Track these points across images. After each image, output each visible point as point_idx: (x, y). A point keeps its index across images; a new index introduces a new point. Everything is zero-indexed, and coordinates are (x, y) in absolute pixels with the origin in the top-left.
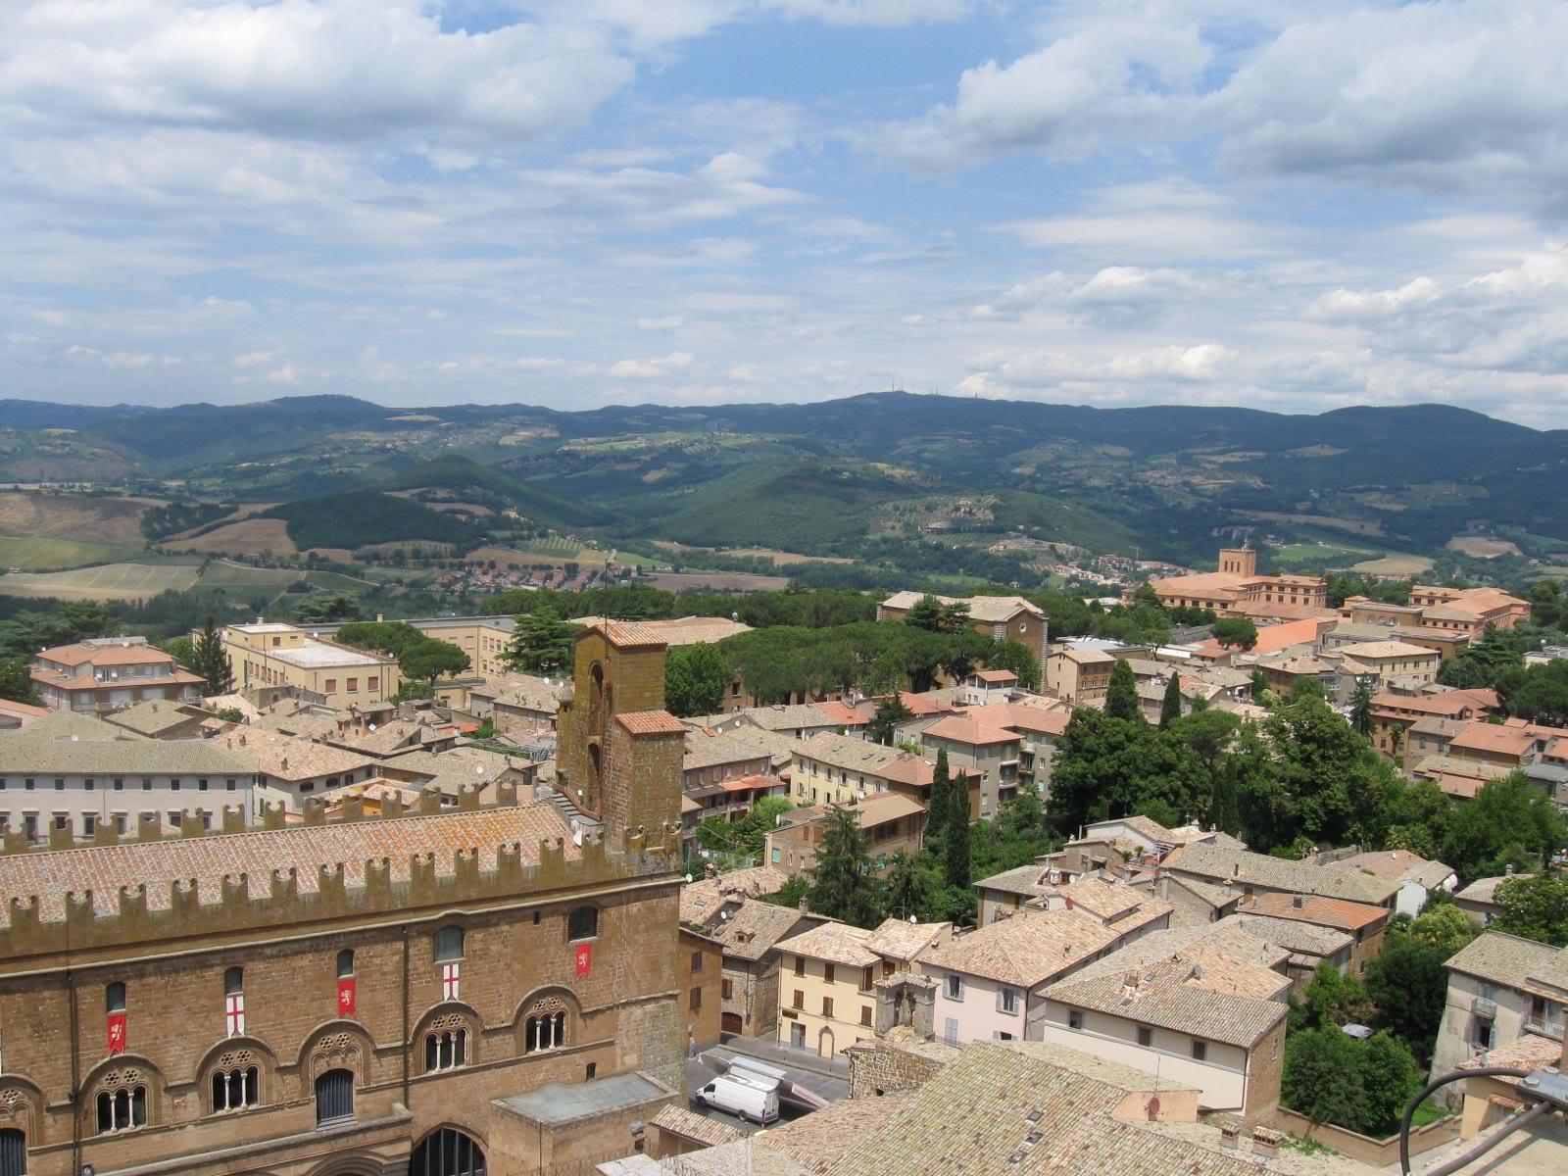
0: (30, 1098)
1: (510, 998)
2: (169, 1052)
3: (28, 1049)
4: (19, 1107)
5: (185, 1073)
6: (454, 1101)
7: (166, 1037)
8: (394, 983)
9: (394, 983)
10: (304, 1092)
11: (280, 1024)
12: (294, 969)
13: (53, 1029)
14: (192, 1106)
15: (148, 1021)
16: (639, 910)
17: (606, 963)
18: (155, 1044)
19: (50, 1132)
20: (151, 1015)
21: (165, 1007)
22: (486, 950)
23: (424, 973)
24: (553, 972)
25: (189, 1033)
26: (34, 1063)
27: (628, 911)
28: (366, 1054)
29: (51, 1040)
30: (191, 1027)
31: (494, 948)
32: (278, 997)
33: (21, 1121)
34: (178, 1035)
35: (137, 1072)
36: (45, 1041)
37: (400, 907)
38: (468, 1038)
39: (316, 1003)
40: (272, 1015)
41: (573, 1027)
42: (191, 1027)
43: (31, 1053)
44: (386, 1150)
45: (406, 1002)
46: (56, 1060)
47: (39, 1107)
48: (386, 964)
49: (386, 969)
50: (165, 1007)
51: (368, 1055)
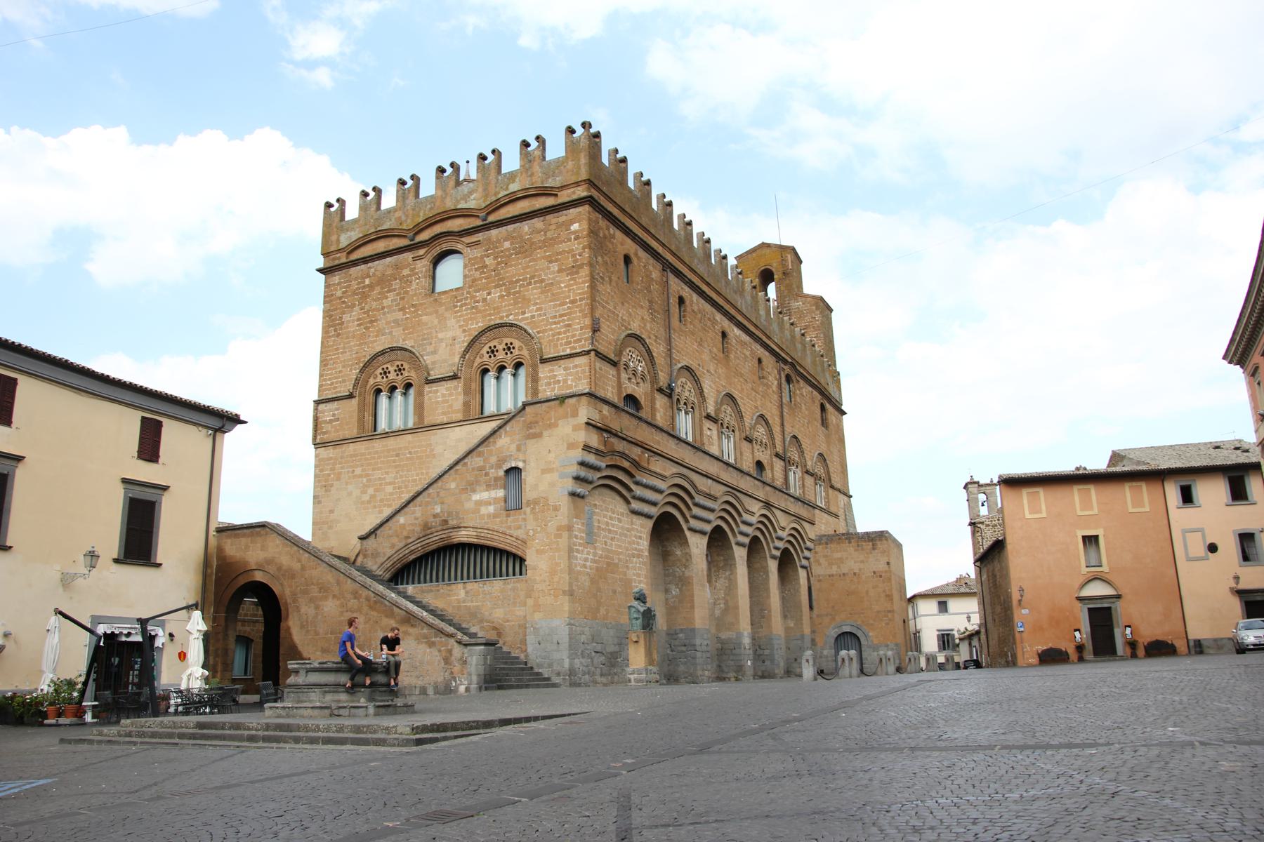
45: (783, 425)
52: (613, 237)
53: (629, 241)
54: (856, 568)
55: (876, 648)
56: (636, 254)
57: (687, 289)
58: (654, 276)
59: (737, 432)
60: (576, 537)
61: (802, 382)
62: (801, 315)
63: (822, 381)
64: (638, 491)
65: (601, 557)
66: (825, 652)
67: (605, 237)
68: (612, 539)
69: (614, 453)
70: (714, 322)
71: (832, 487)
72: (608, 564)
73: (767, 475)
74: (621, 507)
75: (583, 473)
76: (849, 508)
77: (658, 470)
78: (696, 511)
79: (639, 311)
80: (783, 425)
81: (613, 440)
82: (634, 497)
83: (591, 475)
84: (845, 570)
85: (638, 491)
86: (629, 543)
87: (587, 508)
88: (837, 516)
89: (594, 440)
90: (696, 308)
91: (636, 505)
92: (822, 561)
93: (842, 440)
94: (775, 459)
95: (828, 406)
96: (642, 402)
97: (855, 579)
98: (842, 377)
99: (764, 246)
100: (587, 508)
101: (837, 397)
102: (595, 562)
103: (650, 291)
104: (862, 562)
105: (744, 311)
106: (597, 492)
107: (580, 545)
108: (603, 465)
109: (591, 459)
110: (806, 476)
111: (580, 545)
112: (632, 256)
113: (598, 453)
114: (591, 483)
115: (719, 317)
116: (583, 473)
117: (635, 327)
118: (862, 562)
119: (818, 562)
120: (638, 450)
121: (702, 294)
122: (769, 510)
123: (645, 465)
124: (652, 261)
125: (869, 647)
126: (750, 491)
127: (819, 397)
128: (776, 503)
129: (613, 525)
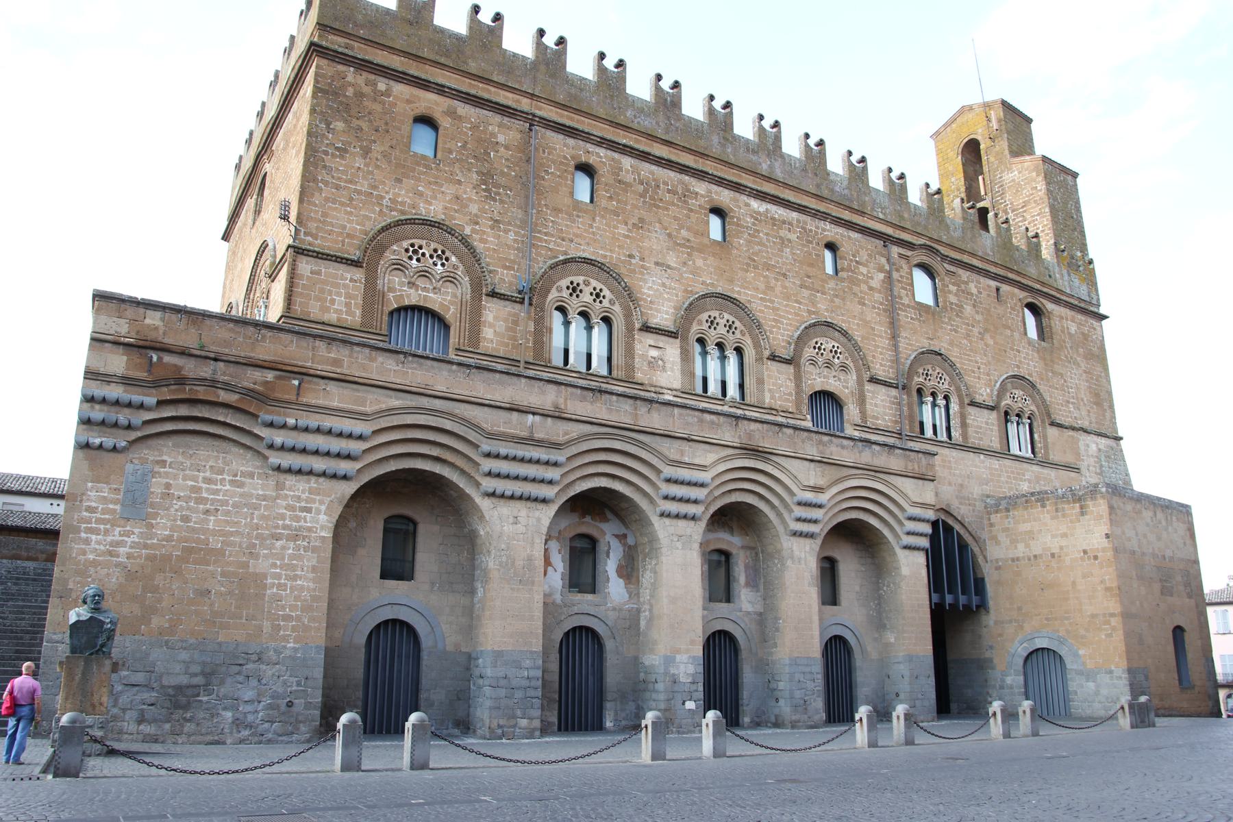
0: (468, 271)
2: (645, 281)
3: (470, 199)
4: (450, 279)
5: (663, 316)
6: (950, 484)
8: (881, 304)
10: (798, 404)
12: (781, 238)
13: (505, 188)
14: (672, 370)
15: (622, 230)
18: (631, 264)
19: (488, 333)
20: (626, 224)
21: (641, 220)
25: (669, 267)
26: (477, 223)
28: (860, 382)
29: (502, 202)
30: (672, 260)
32: (768, 267)
33: (444, 299)
34: (657, 264)
36: (495, 200)
37: (881, 216)
38: (954, 407)
39: (806, 293)
40: (762, 286)
41: (1045, 437)
43: (474, 208)
45: (894, 337)
46: (506, 231)
47: (477, 286)
50: (641, 220)
51: (863, 385)
52: (388, 93)
53: (432, 96)
54: (1054, 544)
55: (1089, 675)
56: (451, 113)
57: (602, 152)
58: (501, 138)
59: (750, 353)
60: (91, 510)
61: (964, 274)
62: (1018, 188)
63: (1032, 271)
64: (279, 438)
65: (169, 539)
66: (1009, 680)
67: (360, 95)
68: (207, 512)
69: (181, 381)
70: (687, 194)
71: (1053, 424)
72: (188, 551)
73: (852, 411)
74: (241, 463)
75: (98, 413)
76: (1115, 456)
77: (335, 404)
78: (488, 465)
79: (450, 190)
80: (894, 337)
81: (168, 359)
82: (271, 446)
83: (123, 417)
84: (1036, 549)
85: (279, 438)
86: (263, 517)
87: (129, 467)
88: (1077, 470)
89: (117, 363)
90: (629, 178)
91: (275, 459)
92: (1002, 537)
93: (1098, 357)
94: (869, 387)
95: (1050, 306)
96: (450, 315)
97: (1054, 564)
98: (1098, 267)
99: (963, 111)
100: (129, 467)
101: (1083, 292)
102: (146, 546)
103: (483, 157)
104: (1064, 535)
105: (779, 174)
106: (170, 442)
107: (99, 521)
108: (151, 400)
109: (115, 392)
110: (971, 410)
111: (99, 521)
112: (437, 115)
113: (127, 381)
114: (129, 427)
115: (701, 187)
116: (98, 413)
117: (434, 209)
118: (1064, 535)
119: (994, 538)
120: (270, 376)
121: (645, 156)
122: (767, 460)
123: (293, 397)
124: (497, 118)
125: (1080, 673)
126: (681, 431)
127: (1022, 294)
128: (782, 448)
129: (216, 492)
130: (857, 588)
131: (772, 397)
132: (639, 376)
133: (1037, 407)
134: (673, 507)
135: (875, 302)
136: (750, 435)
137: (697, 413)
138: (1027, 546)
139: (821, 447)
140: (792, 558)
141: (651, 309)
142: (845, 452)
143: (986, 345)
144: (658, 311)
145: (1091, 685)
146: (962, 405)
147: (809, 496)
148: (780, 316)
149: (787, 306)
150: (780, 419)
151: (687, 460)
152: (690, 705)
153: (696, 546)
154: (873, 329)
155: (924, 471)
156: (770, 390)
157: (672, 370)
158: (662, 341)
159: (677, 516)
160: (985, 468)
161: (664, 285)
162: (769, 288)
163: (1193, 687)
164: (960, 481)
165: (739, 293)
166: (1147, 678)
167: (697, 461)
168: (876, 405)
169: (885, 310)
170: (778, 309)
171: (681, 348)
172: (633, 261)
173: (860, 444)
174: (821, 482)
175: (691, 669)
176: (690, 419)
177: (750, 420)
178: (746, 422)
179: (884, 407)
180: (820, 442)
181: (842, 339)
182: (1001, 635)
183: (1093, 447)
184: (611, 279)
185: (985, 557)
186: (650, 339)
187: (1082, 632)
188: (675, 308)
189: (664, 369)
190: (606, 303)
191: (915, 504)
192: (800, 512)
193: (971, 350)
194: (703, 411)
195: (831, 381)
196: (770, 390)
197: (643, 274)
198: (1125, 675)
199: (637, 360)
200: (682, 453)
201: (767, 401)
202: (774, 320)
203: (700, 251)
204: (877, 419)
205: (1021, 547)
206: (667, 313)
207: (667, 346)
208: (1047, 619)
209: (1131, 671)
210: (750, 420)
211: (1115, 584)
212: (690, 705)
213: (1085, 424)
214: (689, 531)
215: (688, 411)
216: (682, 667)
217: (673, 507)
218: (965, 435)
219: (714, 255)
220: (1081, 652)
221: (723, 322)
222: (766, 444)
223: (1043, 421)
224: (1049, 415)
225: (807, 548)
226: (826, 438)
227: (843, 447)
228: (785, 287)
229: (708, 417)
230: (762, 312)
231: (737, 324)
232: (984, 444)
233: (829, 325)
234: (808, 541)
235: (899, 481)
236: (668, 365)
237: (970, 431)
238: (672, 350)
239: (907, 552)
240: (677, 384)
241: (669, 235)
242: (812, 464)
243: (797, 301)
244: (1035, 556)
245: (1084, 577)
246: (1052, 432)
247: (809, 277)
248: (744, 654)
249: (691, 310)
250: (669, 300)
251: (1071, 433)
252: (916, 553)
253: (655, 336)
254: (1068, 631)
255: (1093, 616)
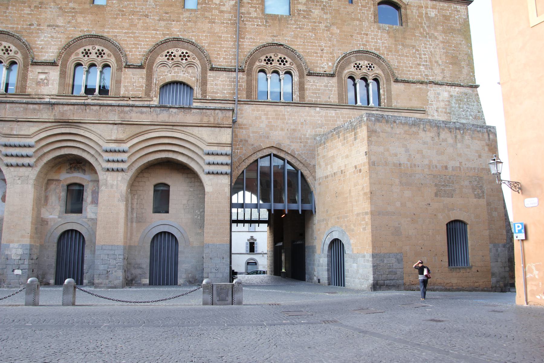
1: (331, 53)
2: (39, 37)
6: (282, 130)
7: (39, 25)
8: (230, 20)
9: (230, 20)
11: (132, 33)
14: (53, 84)
16: (436, 15)
17: (414, 47)
18: (30, 29)
22: (308, 12)
23: (256, 18)
24: (367, 41)
25: (57, 26)
27: (427, 14)
30: (60, 22)
31: (316, 12)
32: (133, 13)
34: (49, 26)
35: (13, 48)
39: (162, 23)
40: (126, 25)
41: (389, 91)
42: (60, 22)
44: (206, 134)
48: (224, 5)
49: (223, 8)
71: (396, 81)
73: (197, 92)
104: (347, 157)
130: (185, 202)
131: (126, 90)
132: (29, 90)
133: (383, 70)
134: (13, 161)
135: (224, 19)
136: (63, 114)
137: (23, 105)
138: (332, 167)
139: (122, 115)
140: (106, 185)
141: (41, 52)
142: (144, 116)
143: (332, 34)
144: (47, 52)
145: (355, 265)
146: (301, 76)
147: (113, 146)
148: (140, 41)
149: (146, 33)
150: (131, 103)
151: (15, 133)
152: (18, 272)
153: (31, 182)
154: (220, 37)
155: (220, 121)
156: (125, 86)
157: (53, 84)
158: (47, 69)
159: (18, 165)
160: (321, 117)
161: (52, 37)
162: (133, 25)
163: (471, 268)
164: (293, 127)
165: (108, 32)
166: (399, 261)
167: (22, 133)
168: (216, 85)
169: (232, 24)
170: (138, 37)
171: (61, 70)
172: (32, 27)
173: (158, 109)
174: (122, 136)
175: (20, 252)
176: (18, 109)
177: (63, 104)
178: (61, 106)
179: (224, 85)
180: (122, 112)
181: (190, 47)
182: (319, 230)
183: (446, 95)
184: (16, 40)
185: (314, 177)
186: (39, 69)
187: (352, 227)
188: (59, 49)
189: (47, 84)
190: (12, 54)
191: (210, 144)
192: (107, 156)
193: (316, 39)
194: (27, 103)
195: (181, 74)
196: (125, 86)
197: (38, 33)
198: (371, 259)
199: (28, 82)
200: (12, 129)
201: (122, 92)
202: (134, 44)
203: (81, 13)
204: (217, 93)
205: (329, 167)
206: (53, 52)
207: (51, 72)
208: (338, 218)
209: (374, 256)
210: (63, 104)
211: (368, 190)
212: (18, 272)
213: (439, 79)
214: (27, 174)
215: (17, 105)
216: (14, 251)
217: (13, 161)
218: (302, 96)
219: (92, 13)
220: (352, 241)
221: (93, 52)
222: (76, 118)
223: (388, 80)
224: (393, 75)
225: (120, 178)
226: (127, 109)
227: (142, 113)
228: (147, 23)
229: (31, 106)
230: (126, 40)
231: (106, 51)
232: (323, 99)
233: (178, 40)
234: (120, 174)
235: (195, 131)
236: (50, 82)
237: (307, 93)
238: (54, 74)
239: (211, 177)
240: (55, 92)
241: (60, 8)
242: (116, 126)
243: (154, 30)
244: (334, 173)
245: (355, 186)
246: (396, 88)
247: (167, 13)
248: (87, 243)
249: (68, 48)
250: (55, 45)
251: (419, 86)
252: (221, 177)
253: (42, 67)
254: (346, 226)
255: (358, 215)
